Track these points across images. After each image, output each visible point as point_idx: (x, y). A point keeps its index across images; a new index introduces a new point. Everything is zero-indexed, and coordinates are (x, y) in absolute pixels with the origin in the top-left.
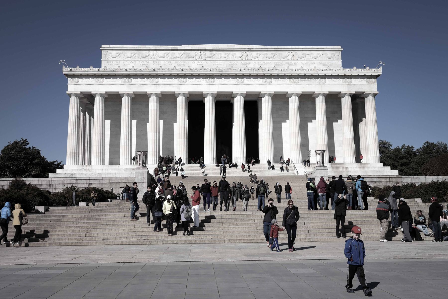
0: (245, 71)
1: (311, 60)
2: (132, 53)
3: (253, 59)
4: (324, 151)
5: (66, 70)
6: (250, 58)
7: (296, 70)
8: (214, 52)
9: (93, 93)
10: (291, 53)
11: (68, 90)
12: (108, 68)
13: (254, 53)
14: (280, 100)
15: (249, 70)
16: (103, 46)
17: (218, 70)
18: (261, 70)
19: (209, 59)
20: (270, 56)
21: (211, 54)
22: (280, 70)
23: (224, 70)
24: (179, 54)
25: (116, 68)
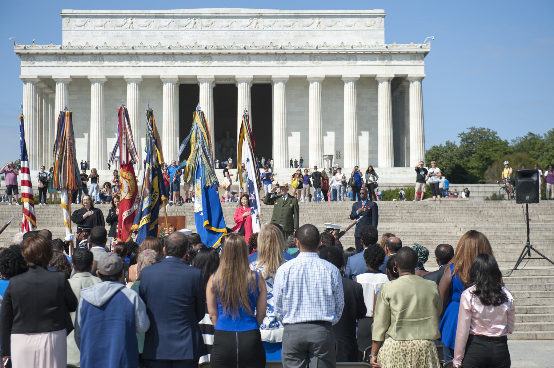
0: (251, 48)
1: (343, 28)
2: (102, 21)
3: (266, 29)
4: (332, 156)
5: (19, 48)
6: (261, 27)
7: (317, 47)
8: (213, 20)
9: (53, 77)
10: (317, 20)
11: (22, 74)
12: (72, 45)
13: (267, 21)
14: (297, 85)
15: (256, 47)
16: (64, 11)
17: (216, 48)
18: (272, 48)
19: (206, 29)
20: (288, 24)
21: (209, 22)
22: (297, 47)
23: (223, 47)
24: (166, 22)
25: (83, 45)
